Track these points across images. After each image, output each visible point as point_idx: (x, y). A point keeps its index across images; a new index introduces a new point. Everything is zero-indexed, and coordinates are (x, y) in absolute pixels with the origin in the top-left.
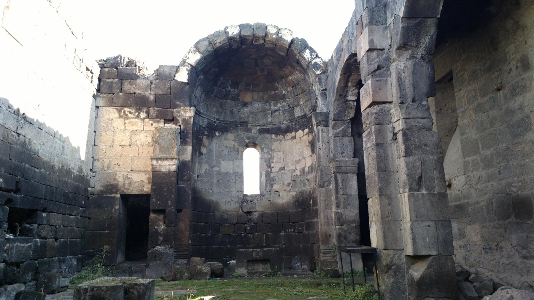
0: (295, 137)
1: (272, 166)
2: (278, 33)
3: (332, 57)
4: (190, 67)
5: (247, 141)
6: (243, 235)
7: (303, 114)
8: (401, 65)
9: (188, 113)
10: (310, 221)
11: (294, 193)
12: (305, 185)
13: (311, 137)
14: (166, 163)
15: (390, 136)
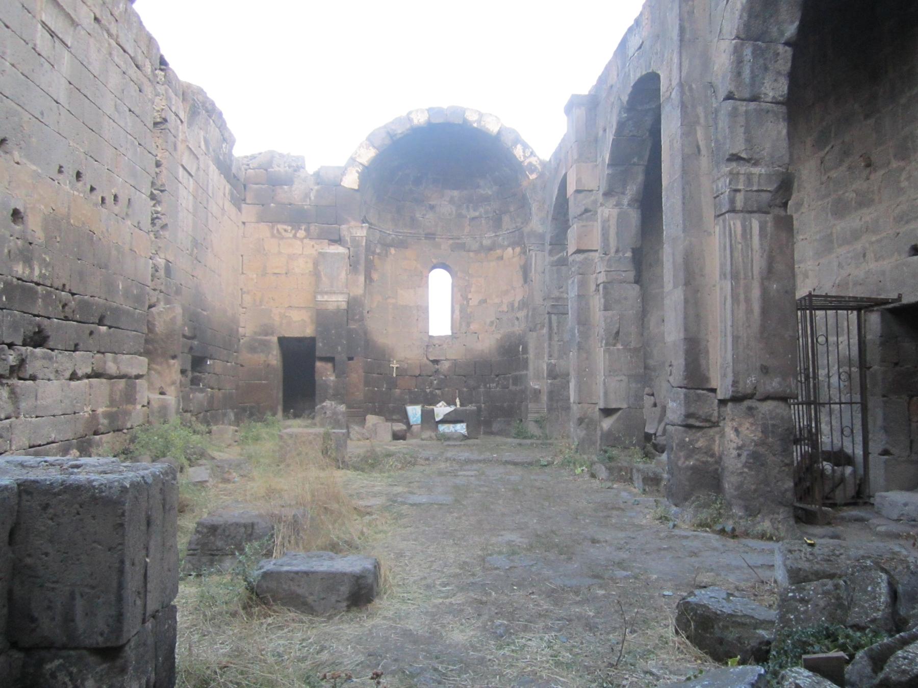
0: (501, 258)
1: (470, 297)
2: (479, 121)
3: (550, 160)
4: (361, 167)
5: (435, 261)
6: (428, 391)
7: (514, 226)
8: (608, 211)
9: (361, 232)
10: (517, 373)
11: (499, 336)
12: (513, 325)
13: (522, 263)
14: (334, 298)
15: (593, 287)
